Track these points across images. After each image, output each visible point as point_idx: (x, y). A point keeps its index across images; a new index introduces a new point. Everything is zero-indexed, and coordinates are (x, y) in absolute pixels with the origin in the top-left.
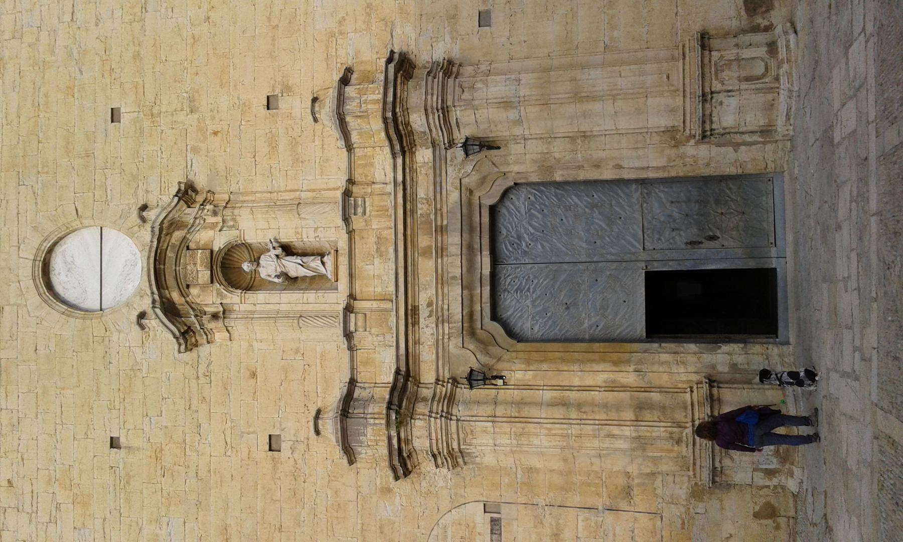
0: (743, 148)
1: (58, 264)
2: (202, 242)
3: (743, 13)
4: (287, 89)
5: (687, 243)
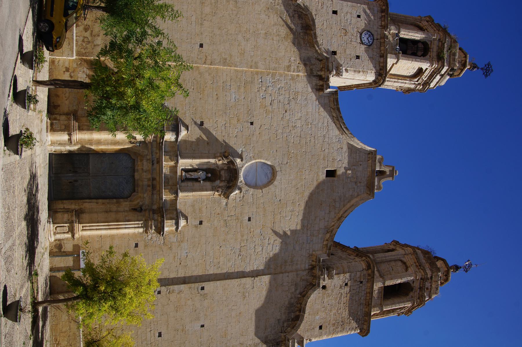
0: (62, 208)
1: (270, 175)
2: (223, 182)
3: (63, 245)
4: (196, 227)
5: (78, 181)
